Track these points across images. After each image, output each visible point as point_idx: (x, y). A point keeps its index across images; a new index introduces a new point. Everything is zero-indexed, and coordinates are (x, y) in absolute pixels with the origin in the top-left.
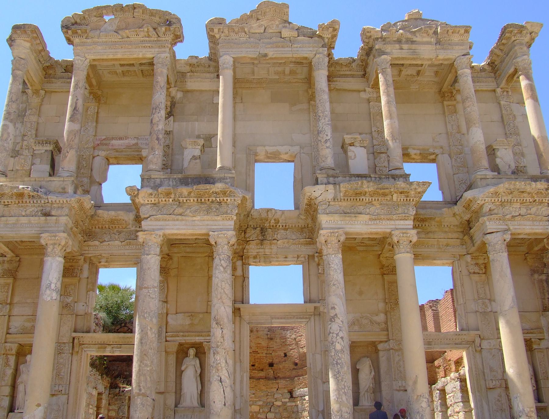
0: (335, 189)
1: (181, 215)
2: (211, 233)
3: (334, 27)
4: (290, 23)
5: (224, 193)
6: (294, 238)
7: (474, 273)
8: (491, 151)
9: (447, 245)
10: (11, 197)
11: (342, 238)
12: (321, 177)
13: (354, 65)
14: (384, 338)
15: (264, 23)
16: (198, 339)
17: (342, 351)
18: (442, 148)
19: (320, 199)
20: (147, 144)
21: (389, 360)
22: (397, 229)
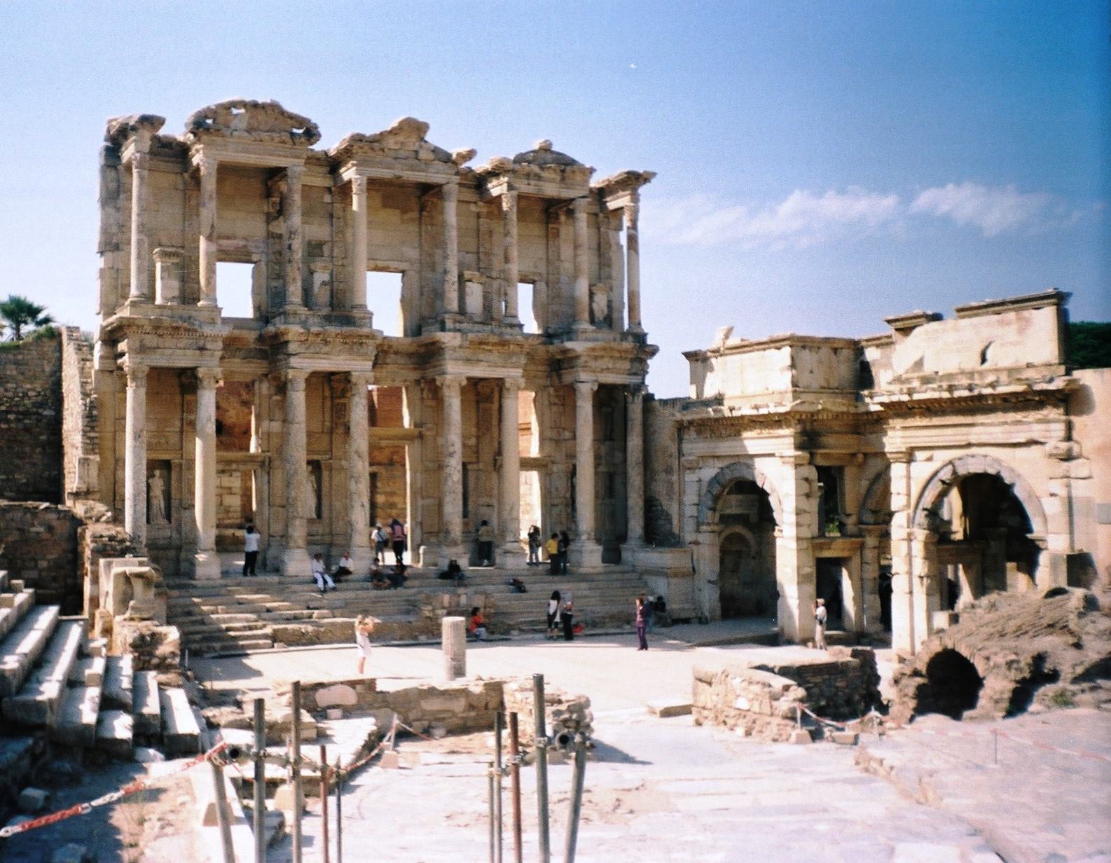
0: (462, 337)
1: (326, 354)
2: (353, 373)
3: (470, 155)
4: (426, 142)
5: (367, 337)
6: (403, 362)
7: (555, 404)
8: (591, 295)
9: (535, 377)
10: (167, 328)
11: (464, 383)
12: (449, 324)
13: (470, 175)
14: (474, 460)
15: (401, 138)
16: (316, 457)
17: (458, 482)
18: (540, 274)
19: (448, 345)
20: (258, 248)
21: (477, 478)
22: (510, 377)
